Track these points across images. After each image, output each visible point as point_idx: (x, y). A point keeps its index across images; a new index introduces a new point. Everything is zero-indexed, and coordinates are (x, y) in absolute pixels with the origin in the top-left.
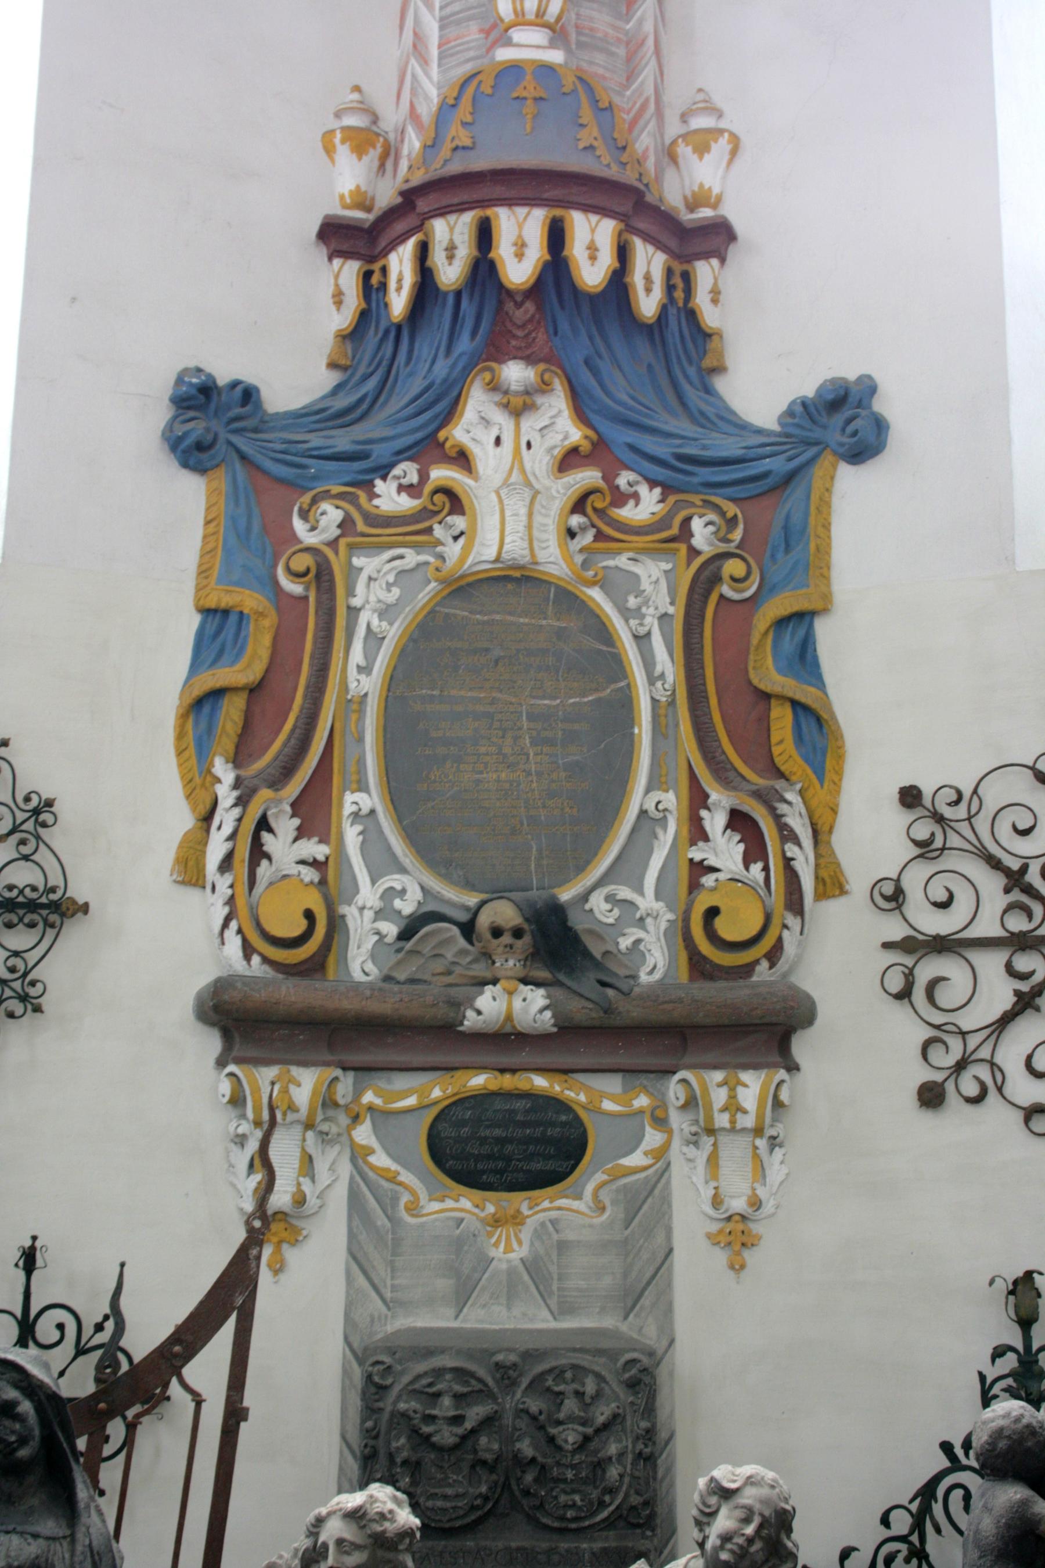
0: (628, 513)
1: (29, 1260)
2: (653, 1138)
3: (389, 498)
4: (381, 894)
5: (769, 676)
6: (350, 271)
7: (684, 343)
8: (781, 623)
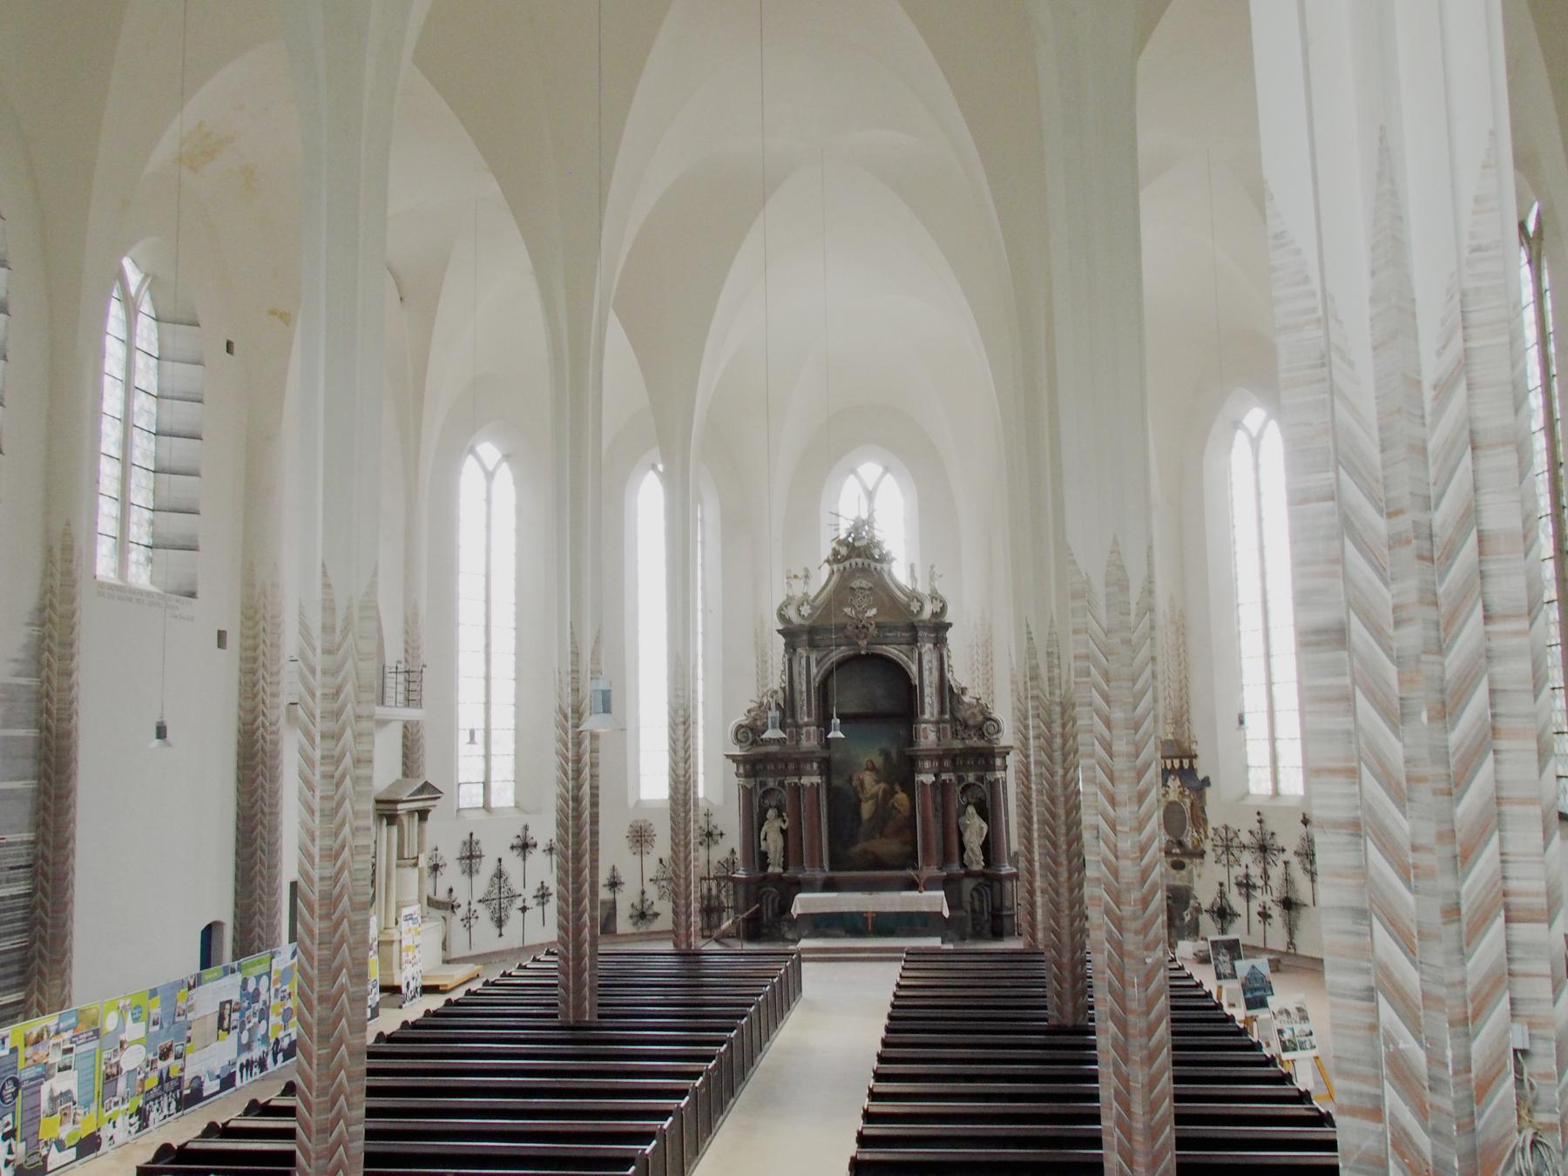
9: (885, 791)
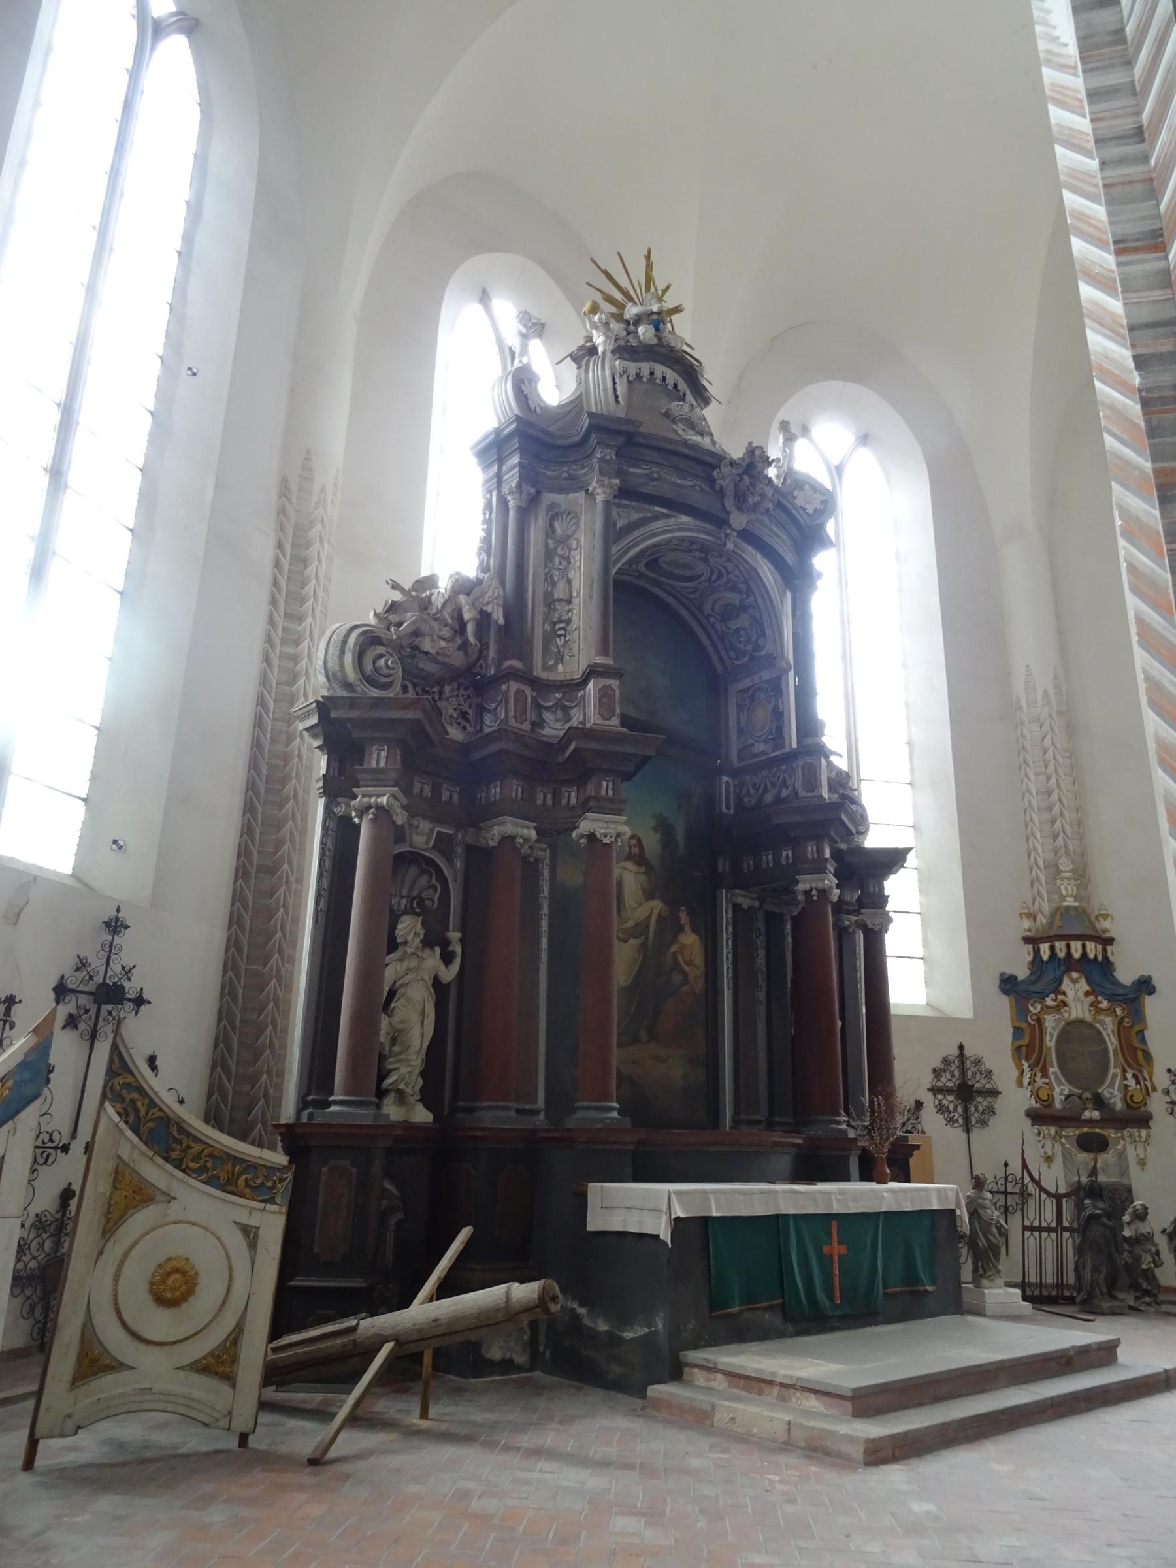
0: (1100, 1006)
1: (1006, 1165)
2: (1122, 1142)
3: (1049, 1002)
4: (1060, 1091)
5: (1137, 1044)
6: (1030, 946)
7: (1106, 966)
8: (1138, 1032)
9: (660, 918)
